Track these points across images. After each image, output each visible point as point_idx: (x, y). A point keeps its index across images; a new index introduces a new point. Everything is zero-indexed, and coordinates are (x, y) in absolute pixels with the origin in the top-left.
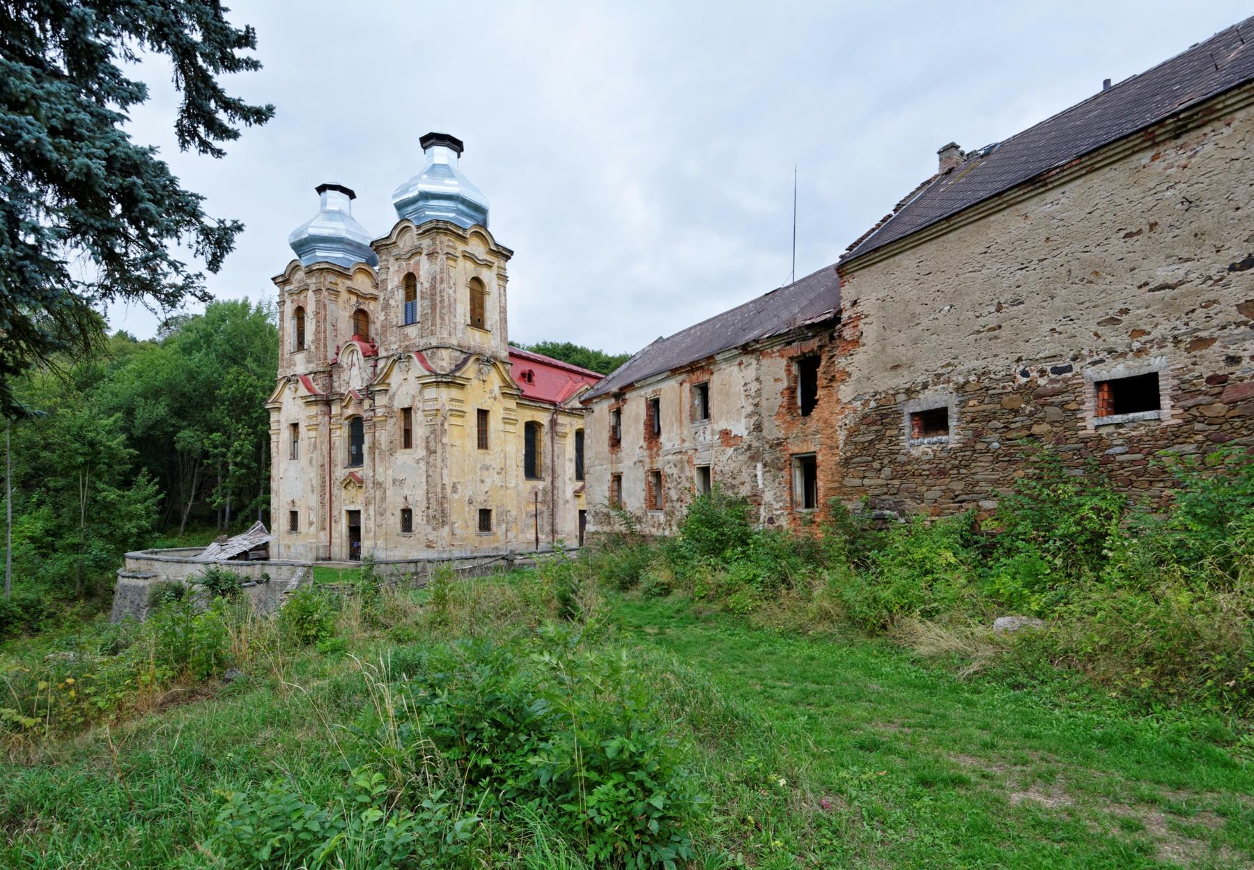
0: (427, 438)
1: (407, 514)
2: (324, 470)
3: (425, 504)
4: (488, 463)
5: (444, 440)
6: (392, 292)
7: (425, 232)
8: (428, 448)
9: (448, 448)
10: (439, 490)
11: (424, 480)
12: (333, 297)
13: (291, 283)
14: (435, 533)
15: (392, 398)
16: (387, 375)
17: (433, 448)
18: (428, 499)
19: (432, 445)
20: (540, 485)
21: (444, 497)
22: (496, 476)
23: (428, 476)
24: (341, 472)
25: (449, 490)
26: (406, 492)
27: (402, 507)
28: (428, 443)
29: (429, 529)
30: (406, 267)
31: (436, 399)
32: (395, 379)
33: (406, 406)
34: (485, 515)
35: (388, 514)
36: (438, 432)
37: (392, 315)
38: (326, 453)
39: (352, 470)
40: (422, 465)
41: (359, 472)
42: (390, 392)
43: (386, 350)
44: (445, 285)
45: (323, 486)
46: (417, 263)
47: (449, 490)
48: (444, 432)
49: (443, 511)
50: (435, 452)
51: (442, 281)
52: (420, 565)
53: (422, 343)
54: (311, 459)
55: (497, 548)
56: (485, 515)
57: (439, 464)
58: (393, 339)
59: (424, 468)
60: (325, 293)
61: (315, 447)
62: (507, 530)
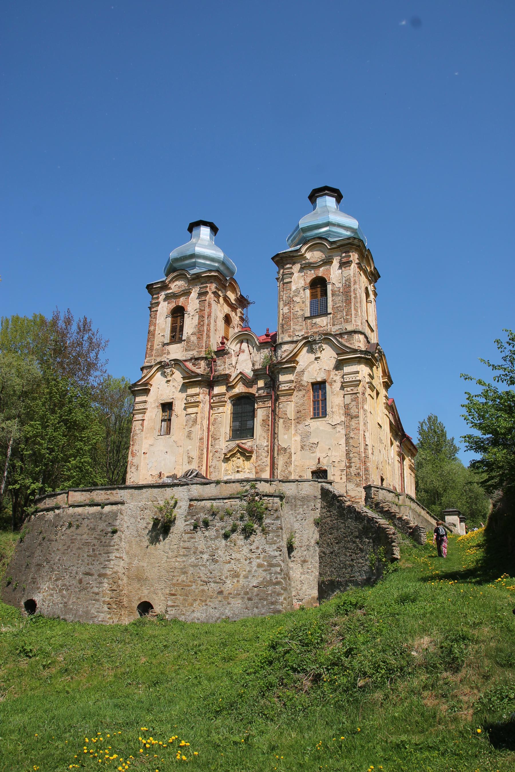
5: (366, 407)
6: (297, 291)
7: (339, 247)
8: (347, 414)
9: (368, 414)
10: (362, 450)
11: (343, 441)
12: (216, 299)
13: (170, 289)
16: (296, 355)
19: (353, 411)
21: (366, 457)
23: (348, 438)
26: (318, 455)
27: (314, 468)
30: (311, 275)
31: (358, 372)
32: (305, 358)
33: (319, 379)
36: (360, 400)
37: (297, 308)
39: (237, 442)
40: (341, 430)
41: (247, 444)
42: (298, 369)
43: (290, 336)
44: (357, 286)
45: (200, 458)
46: (329, 271)
47: (370, 451)
48: (365, 400)
49: (366, 470)
50: (357, 417)
51: (355, 283)
52: (400, 497)
53: (334, 330)
54: (190, 432)
57: (362, 427)
58: (298, 328)
59: (343, 432)
60: (211, 295)
61: (195, 421)
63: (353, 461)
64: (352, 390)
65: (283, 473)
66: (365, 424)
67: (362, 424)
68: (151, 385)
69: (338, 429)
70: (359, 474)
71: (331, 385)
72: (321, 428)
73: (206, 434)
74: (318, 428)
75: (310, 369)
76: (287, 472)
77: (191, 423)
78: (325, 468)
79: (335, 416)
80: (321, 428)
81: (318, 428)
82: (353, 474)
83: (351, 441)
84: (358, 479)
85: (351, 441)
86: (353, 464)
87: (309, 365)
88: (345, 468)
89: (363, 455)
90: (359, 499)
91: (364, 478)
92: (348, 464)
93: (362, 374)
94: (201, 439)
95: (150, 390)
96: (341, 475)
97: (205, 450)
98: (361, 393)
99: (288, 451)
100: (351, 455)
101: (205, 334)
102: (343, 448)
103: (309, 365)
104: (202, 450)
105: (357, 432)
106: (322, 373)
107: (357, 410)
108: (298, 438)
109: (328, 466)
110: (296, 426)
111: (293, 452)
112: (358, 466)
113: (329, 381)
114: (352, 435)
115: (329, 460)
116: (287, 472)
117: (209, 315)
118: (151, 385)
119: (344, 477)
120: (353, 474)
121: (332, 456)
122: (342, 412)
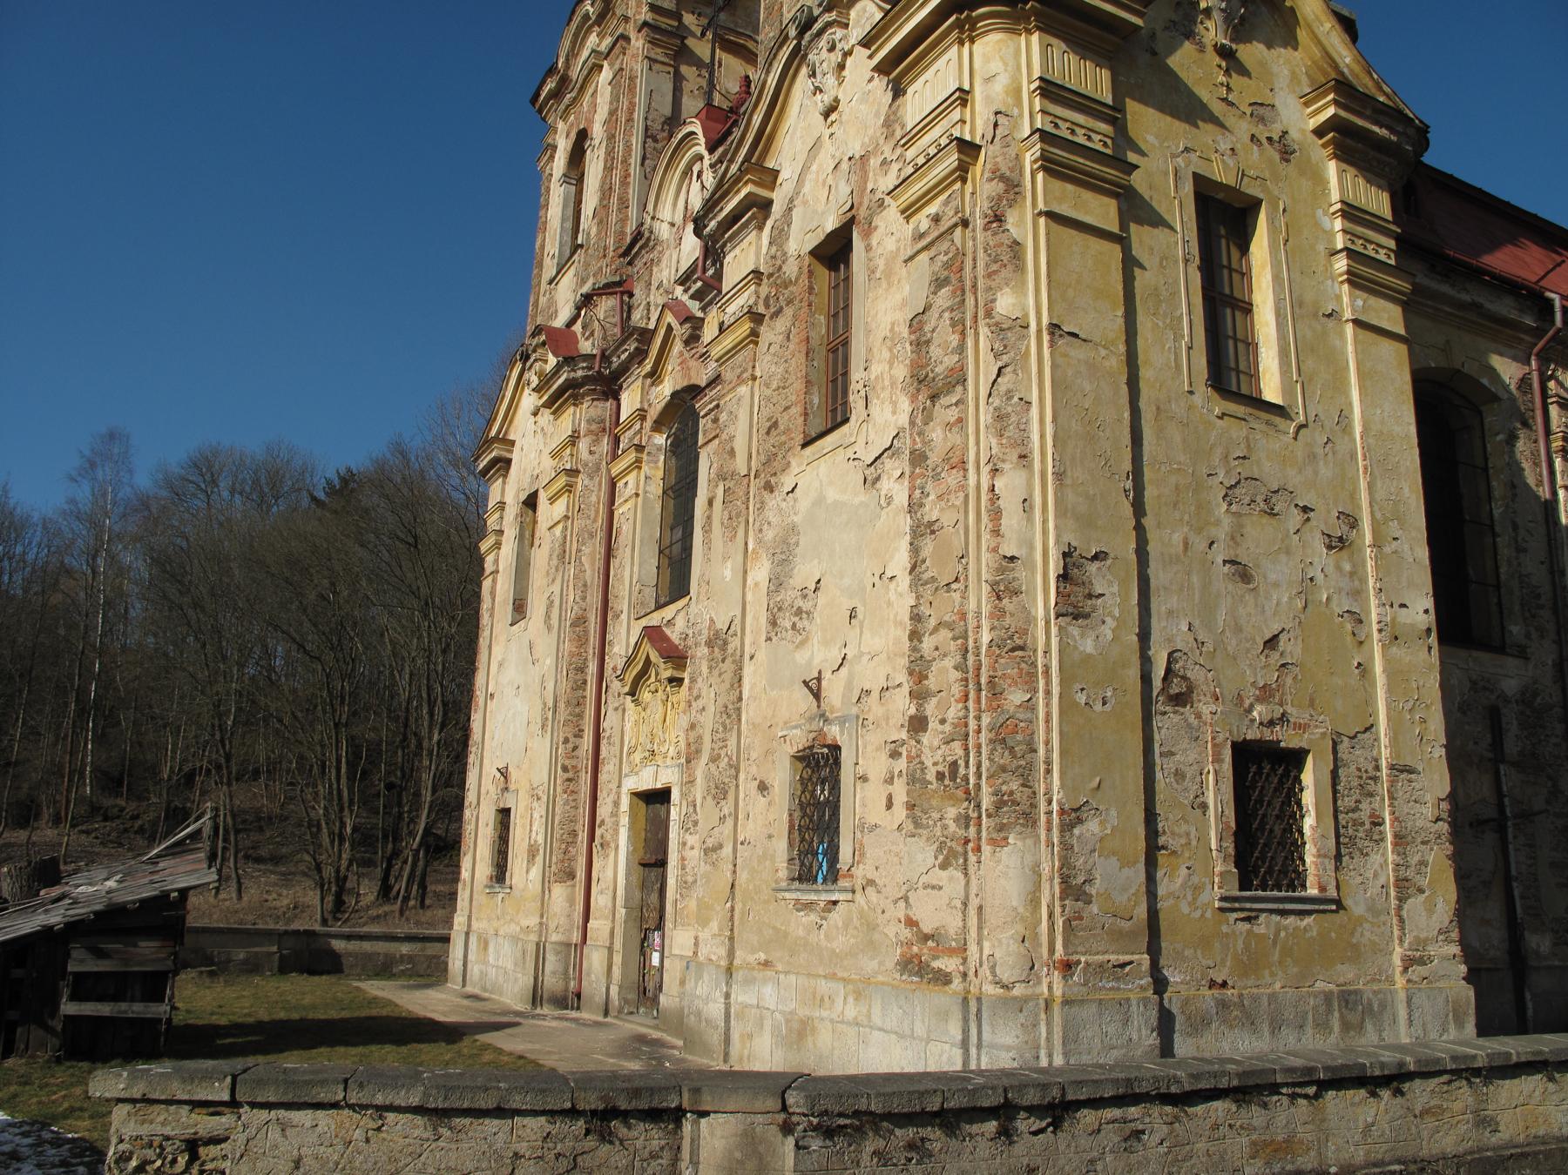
0: (916, 322)
1: (820, 766)
2: (582, 641)
3: (902, 704)
4: (1269, 470)
10: (979, 600)
11: (900, 561)
14: (951, 880)
15: (779, 238)
17: (942, 360)
18: (918, 671)
20: (1511, 677)
22: (1320, 555)
24: (624, 637)
25: (1042, 599)
26: (817, 655)
27: (799, 739)
28: (921, 344)
29: (923, 854)
33: (831, 224)
34: (1264, 771)
35: (747, 787)
38: (592, 575)
42: (777, 210)
50: (958, 378)
55: (1347, 998)
56: (1264, 771)
59: (901, 498)
62: (1404, 887)
63: (932, 683)
64: (936, 219)
65: (713, 767)
66: (1000, 417)
67: (985, 417)
68: (513, 443)
69: (886, 485)
70: (954, 765)
71: (868, 232)
72: (832, 495)
73: (595, 598)
74: (820, 501)
75: (806, 189)
76: (724, 763)
77: (555, 562)
78: (834, 732)
79: (875, 409)
80: (832, 495)
81: (820, 501)
82: (931, 776)
83: (928, 547)
84: (951, 812)
85: (928, 547)
86: (930, 708)
87: (805, 169)
88: (904, 735)
89: (986, 638)
90: (951, 952)
91: (986, 802)
92: (913, 711)
93: (988, 99)
94: (580, 621)
95: (509, 462)
96: (890, 780)
97: (592, 668)
98: (980, 223)
99: (734, 643)
100: (927, 644)
101: (614, 200)
102: (901, 598)
103: (805, 169)
104: (581, 670)
105: (952, 478)
106: (842, 184)
107: (954, 339)
108: (760, 573)
109: (842, 721)
110: (762, 506)
111: (748, 650)
112: (953, 712)
113: (862, 213)
114: (931, 512)
115: (849, 686)
116: (724, 763)
117: (630, 120)
118: (513, 443)
119: (900, 791)
120: (931, 776)
121: (862, 654)
122: (901, 372)
